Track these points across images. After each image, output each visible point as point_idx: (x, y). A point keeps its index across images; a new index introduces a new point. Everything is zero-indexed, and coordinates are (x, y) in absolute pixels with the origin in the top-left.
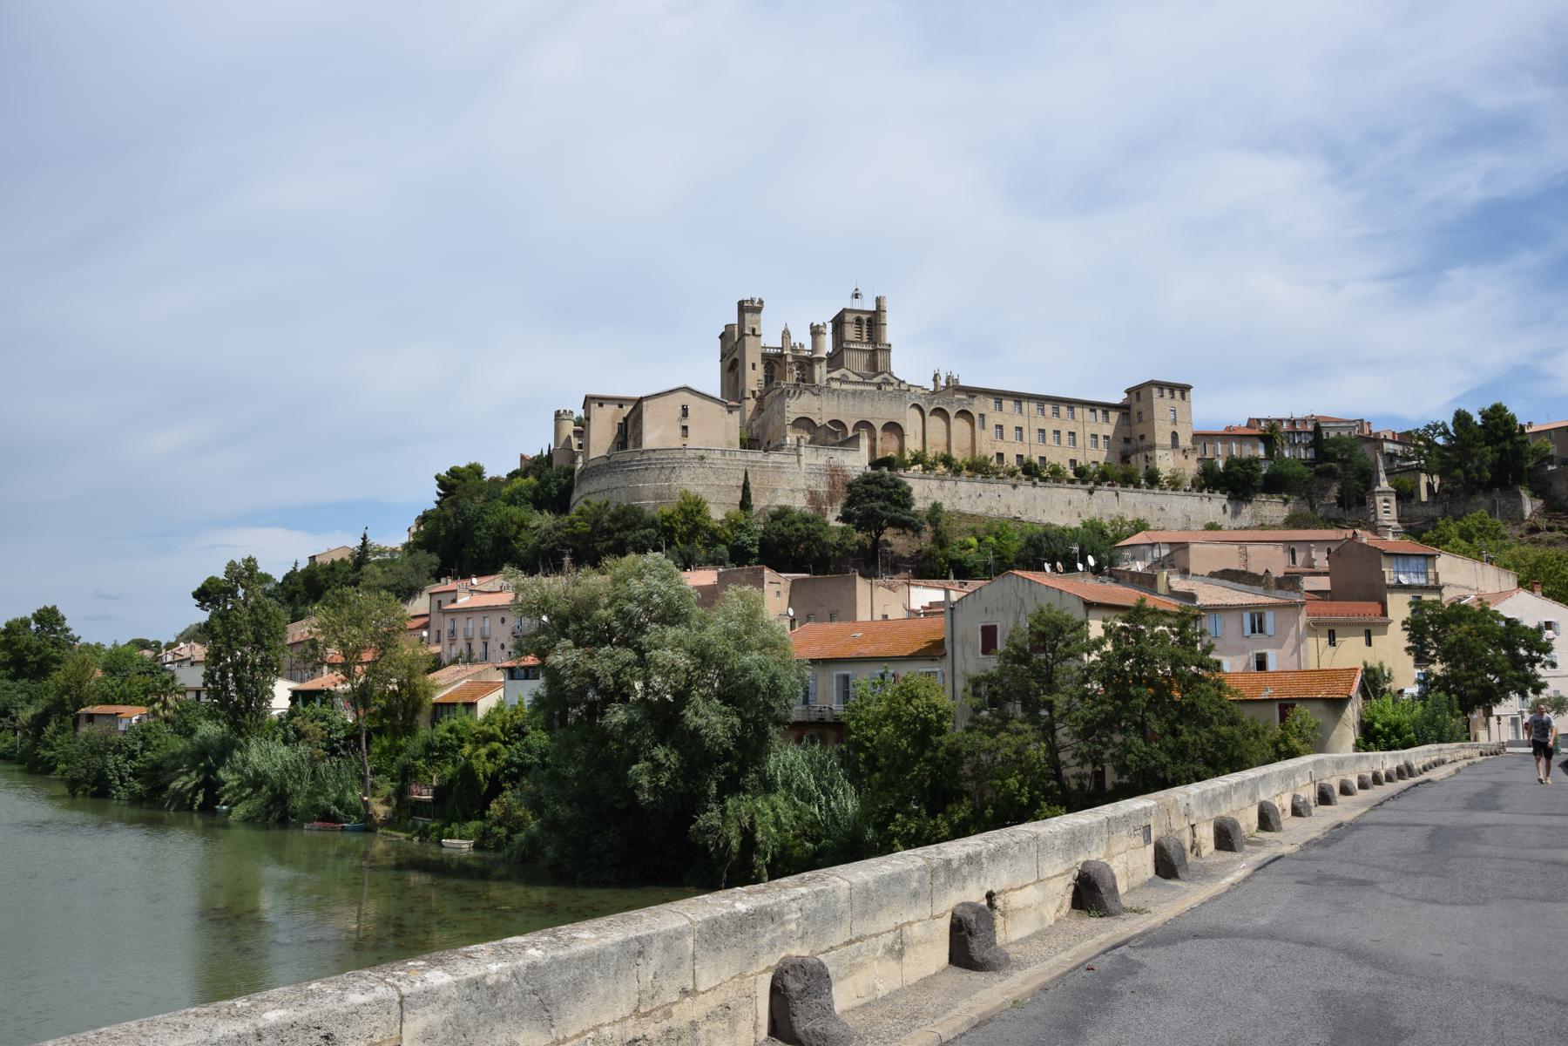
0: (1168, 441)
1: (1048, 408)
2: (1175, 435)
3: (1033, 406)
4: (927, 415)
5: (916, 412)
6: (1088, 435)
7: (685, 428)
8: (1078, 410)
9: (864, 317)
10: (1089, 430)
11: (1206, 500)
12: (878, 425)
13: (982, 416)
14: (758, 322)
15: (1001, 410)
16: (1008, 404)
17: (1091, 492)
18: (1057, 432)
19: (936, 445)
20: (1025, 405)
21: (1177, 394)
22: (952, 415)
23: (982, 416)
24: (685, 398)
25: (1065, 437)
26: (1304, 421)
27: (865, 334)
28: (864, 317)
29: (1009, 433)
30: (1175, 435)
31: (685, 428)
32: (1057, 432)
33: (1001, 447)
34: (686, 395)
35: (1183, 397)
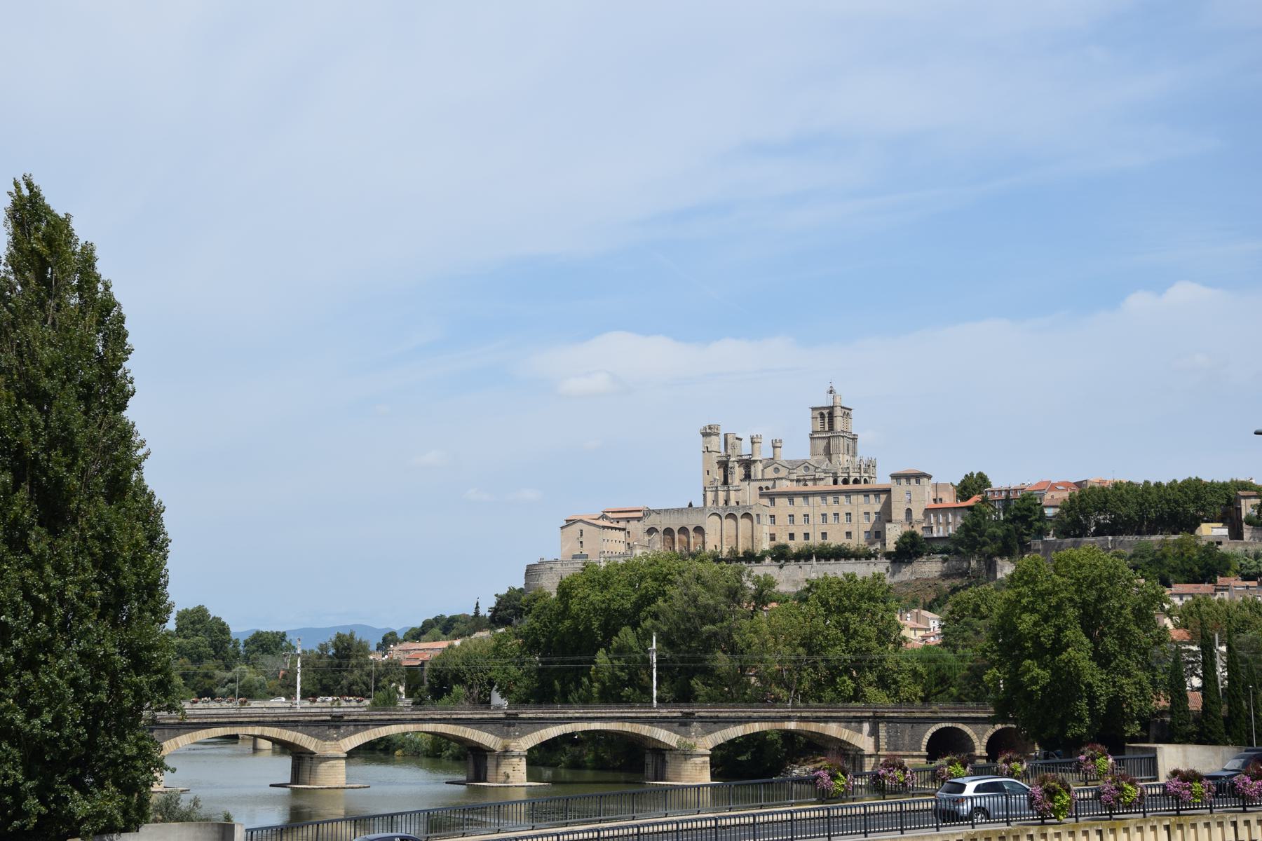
0: (903, 516)
1: (830, 499)
2: (909, 511)
3: (818, 499)
4: (723, 518)
5: (716, 518)
6: (862, 513)
7: (581, 542)
8: (854, 497)
9: (825, 412)
10: (862, 510)
11: (872, 565)
12: (691, 529)
13: (758, 515)
14: (710, 442)
15: (793, 504)
16: (799, 501)
17: (781, 567)
18: (836, 514)
19: (730, 537)
20: (811, 499)
21: (913, 481)
22: (739, 516)
23: (758, 515)
24: (580, 525)
25: (843, 518)
26: (1016, 490)
27: (827, 425)
28: (825, 412)
29: (799, 519)
30: (909, 511)
31: (581, 542)
32: (836, 514)
33: (792, 529)
34: (581, 524)
35: (918, 482)
